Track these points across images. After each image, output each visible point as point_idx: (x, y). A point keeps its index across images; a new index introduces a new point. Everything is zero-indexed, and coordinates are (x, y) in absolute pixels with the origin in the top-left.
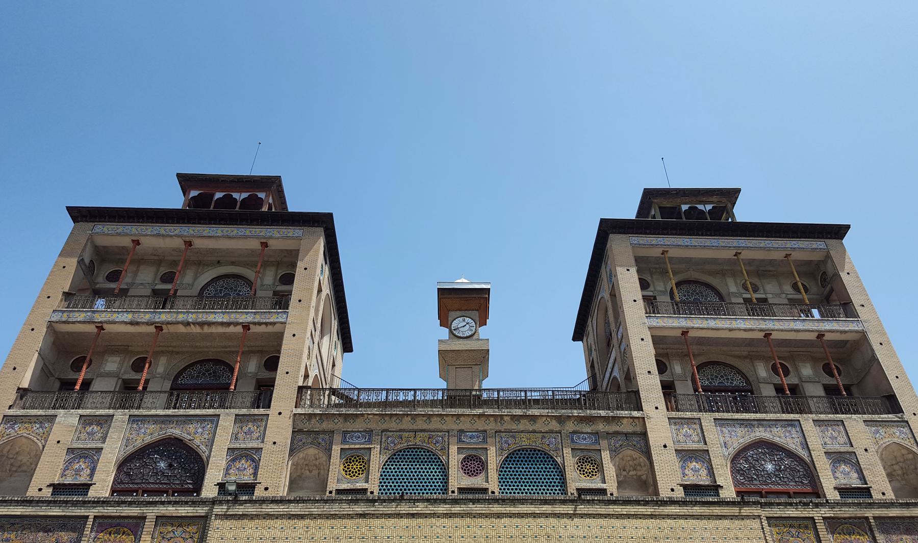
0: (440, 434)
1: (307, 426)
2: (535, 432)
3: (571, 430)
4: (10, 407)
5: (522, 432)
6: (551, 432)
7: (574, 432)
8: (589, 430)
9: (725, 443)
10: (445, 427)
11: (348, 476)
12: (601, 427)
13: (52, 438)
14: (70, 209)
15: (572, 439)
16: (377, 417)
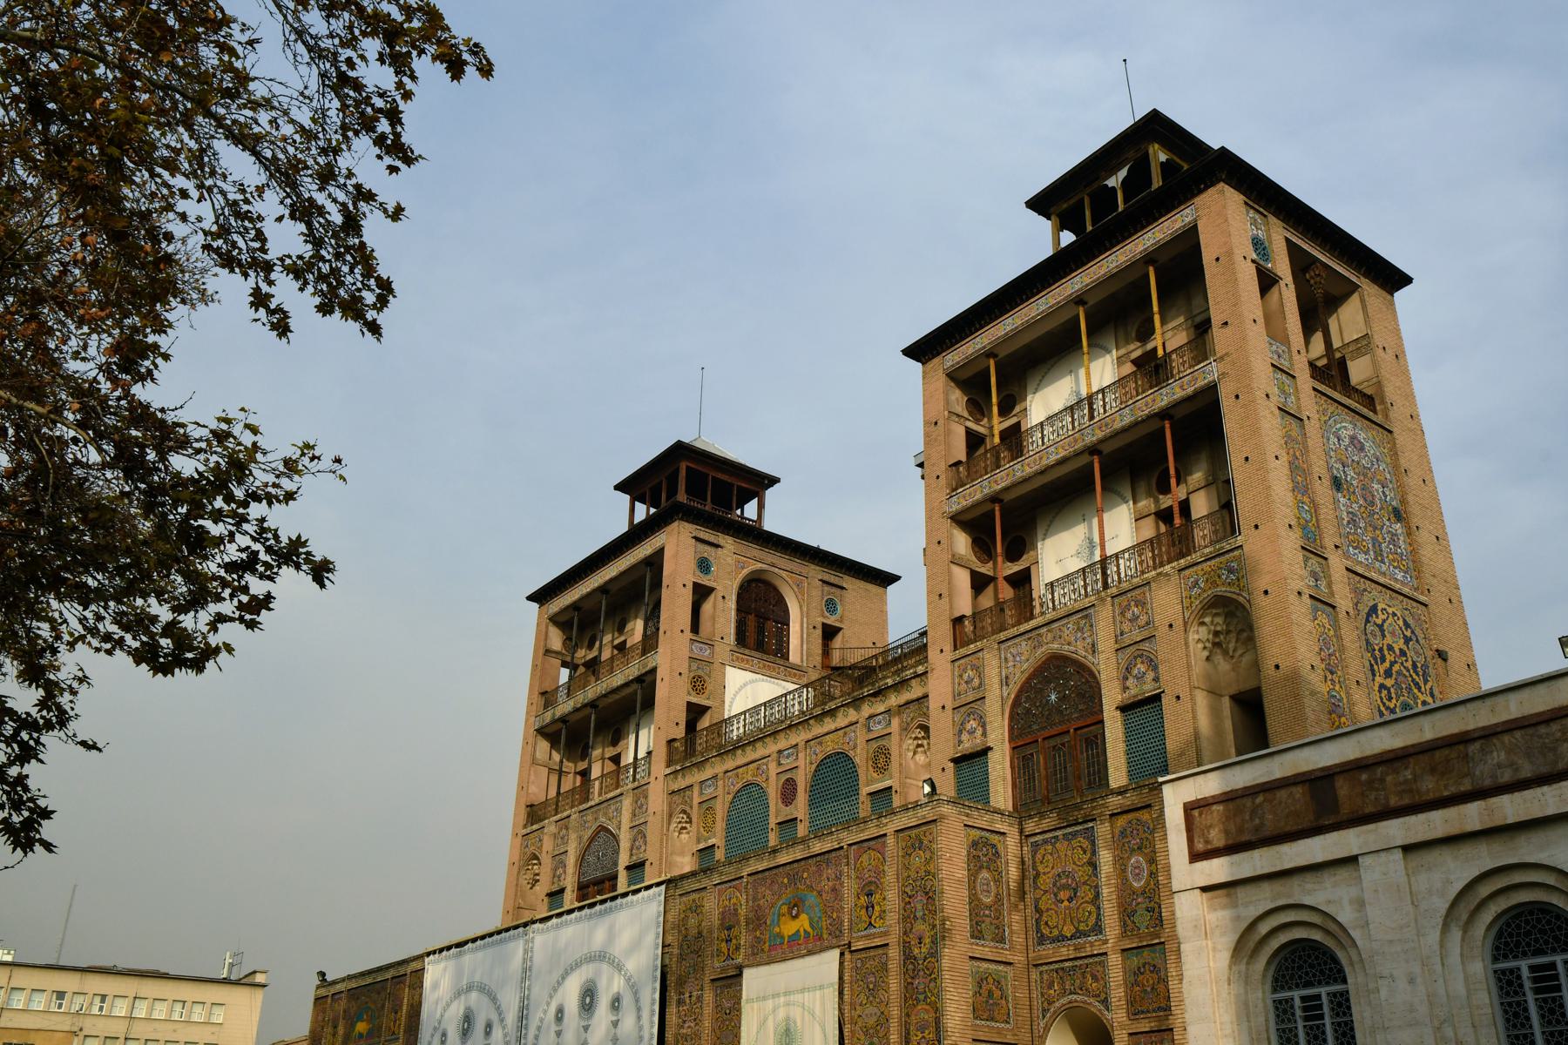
0: (765, 761)
1: (676, 787)
2: (837, 730)
3: (867, 715)
4: (525, 827)
5: (827, 734)
6: (852, 724)
7: (871, 717)
8: (882, 708)
9: (1007, 678)
10: (767, 752)
11: (705, 833)
12: (894, 700)
13: (545, 849)
14: (531, 598)
15: (869, 730)
16: (718, 758)
